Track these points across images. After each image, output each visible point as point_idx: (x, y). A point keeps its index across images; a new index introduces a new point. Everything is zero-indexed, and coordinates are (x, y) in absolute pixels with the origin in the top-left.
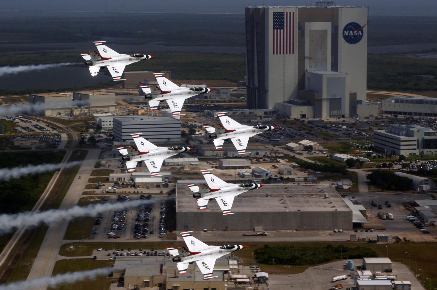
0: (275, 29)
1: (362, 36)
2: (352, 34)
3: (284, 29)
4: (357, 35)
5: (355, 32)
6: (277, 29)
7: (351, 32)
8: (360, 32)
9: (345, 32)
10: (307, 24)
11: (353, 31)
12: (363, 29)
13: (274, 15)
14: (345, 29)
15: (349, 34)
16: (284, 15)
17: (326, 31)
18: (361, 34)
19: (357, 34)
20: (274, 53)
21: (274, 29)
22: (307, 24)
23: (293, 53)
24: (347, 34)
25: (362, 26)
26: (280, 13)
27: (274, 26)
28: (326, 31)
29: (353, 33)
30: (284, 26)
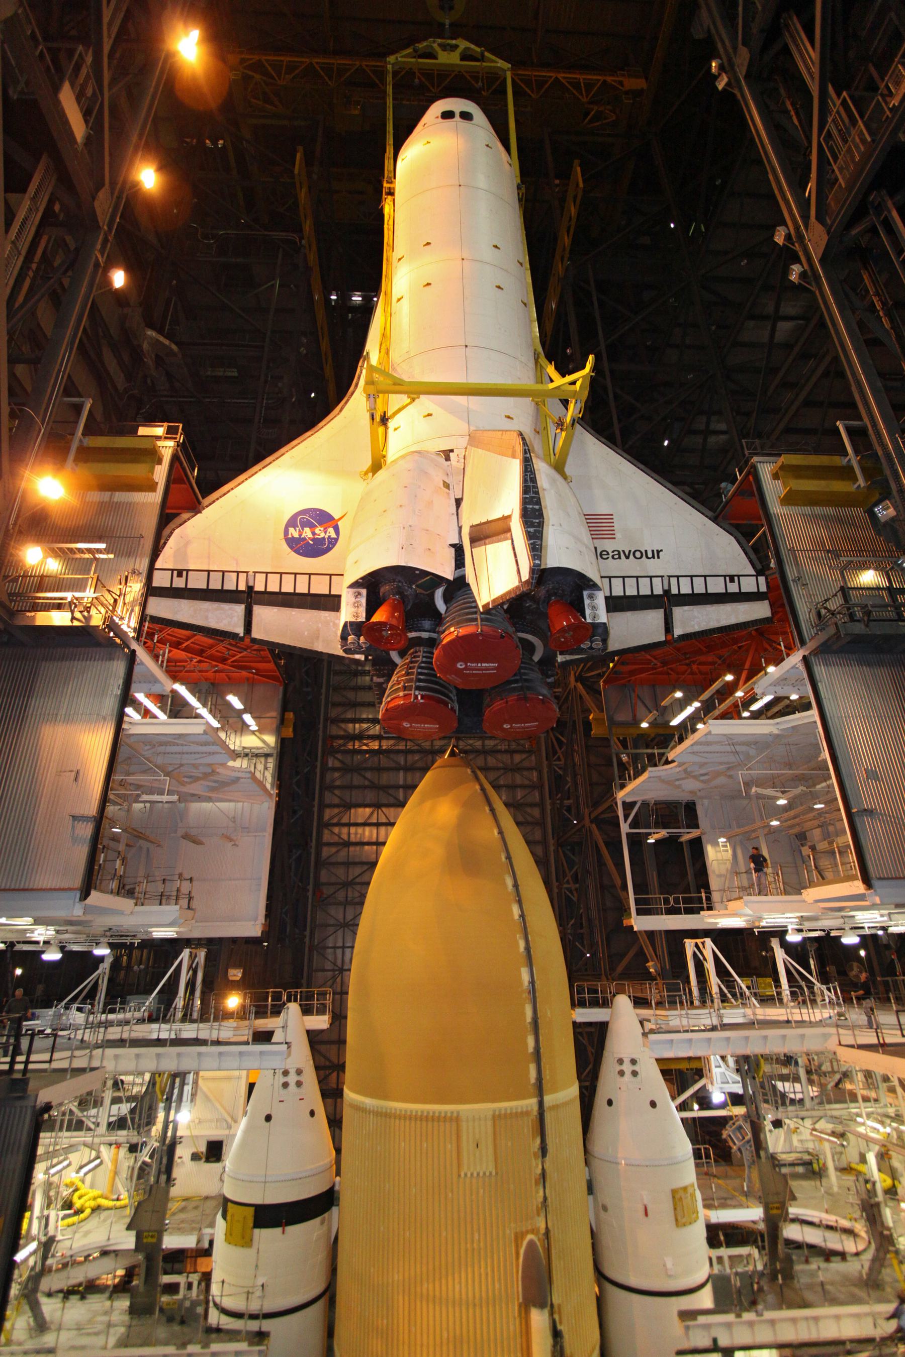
1: (336, 540)
2: (311, 536)
4: (324, 538)
5: (317, 531)
7: (307, 530)
9: (291, 530)
11: (312, 527)
12: (339, 523)
15: (300, 535)
18: (333, 535)
19: (322, 535)
24: (296, 535)
25: (336, 517)
29: (314, 533)
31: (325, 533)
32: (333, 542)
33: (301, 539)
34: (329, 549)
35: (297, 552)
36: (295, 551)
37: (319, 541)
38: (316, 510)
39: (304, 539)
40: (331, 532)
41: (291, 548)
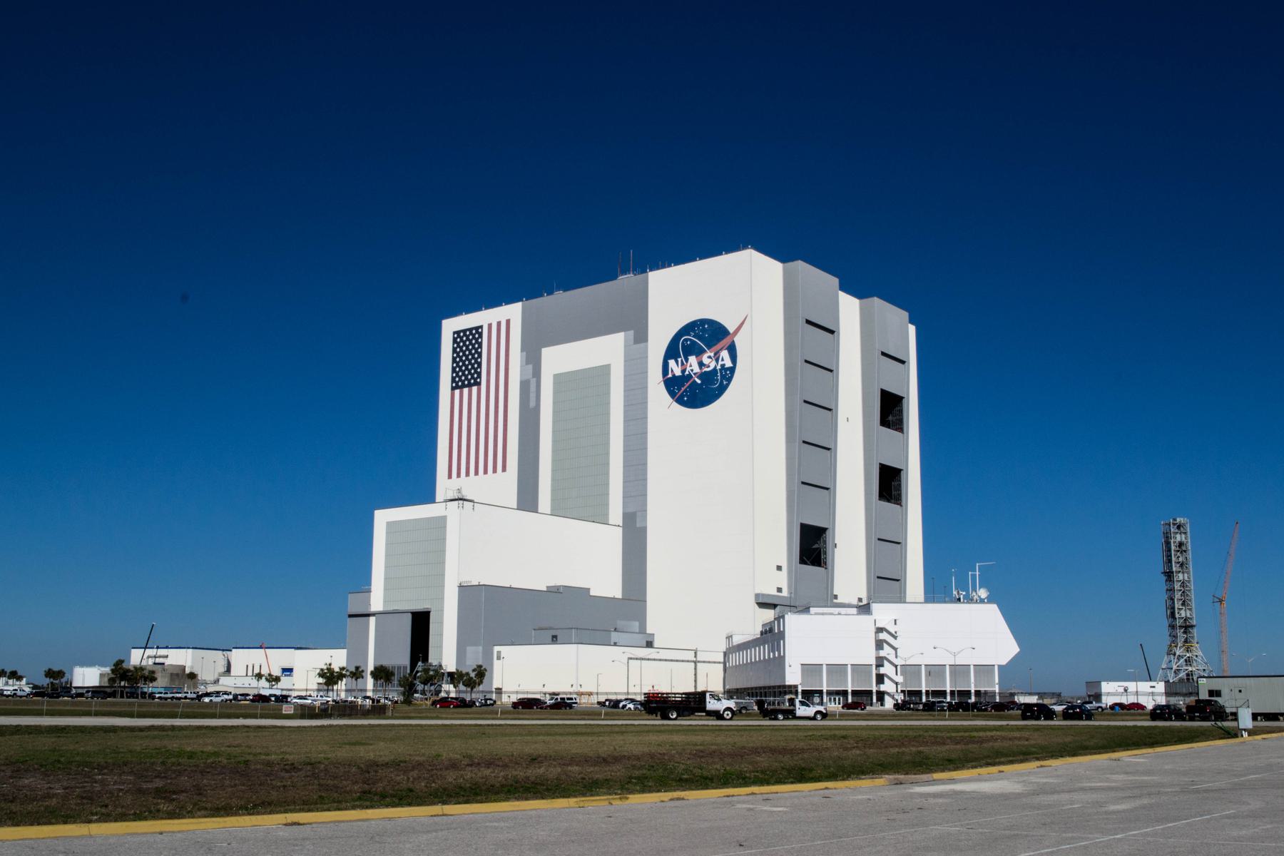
0: (457, 387)
1: (732, 370)
2: (696, 369)
3: (479, 384)
5: (705, 360)
6: (464, 386)
7: (693, 359)
8: (725, 354)
9: (672, 363)
10: (546, 352)
11: (699, 352)
12: (736, 339)
13: (455, 341)
14: (672, 352)
15: (683, 371)
16: (481, 335)
17: (605, 371)
18: (728, 364)
20: (450, 477)
21: (453, 389)
22: (546, 352)
23: (504, 469)
24: (678, 372)
25: (731, 330)
26: (470, 330)
27: (453, 380)
28: (605, 371)
29: (701, 364)
30: (479, 375)
31: (717, 360)
32: (728, 374)
33: (685, 378)
34: (722, 389)
35: (680, 401)
37: (708, 377)
38: (703, 322)
39: (690, 376)
41: (672, 394)
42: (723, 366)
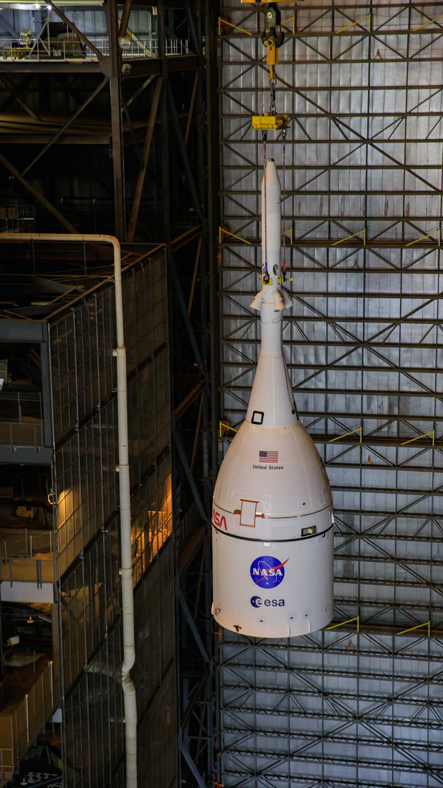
1: (282, 577)
2: (266, 574)
5: (270, 571)
7: (264, 570)
8: (279, 571)
9: (255, 570)
12: (284, 566)
15: (260, 574)
18: (281, 574)
19: (274, 574)
24: (258, 574)
25: (282, 562)
29: (268, 573)
31: (276, 573)
33: (260, 577)
36: (257, 584)
39: (263, 576)
40: (279, 572)
42: (278, 575)
